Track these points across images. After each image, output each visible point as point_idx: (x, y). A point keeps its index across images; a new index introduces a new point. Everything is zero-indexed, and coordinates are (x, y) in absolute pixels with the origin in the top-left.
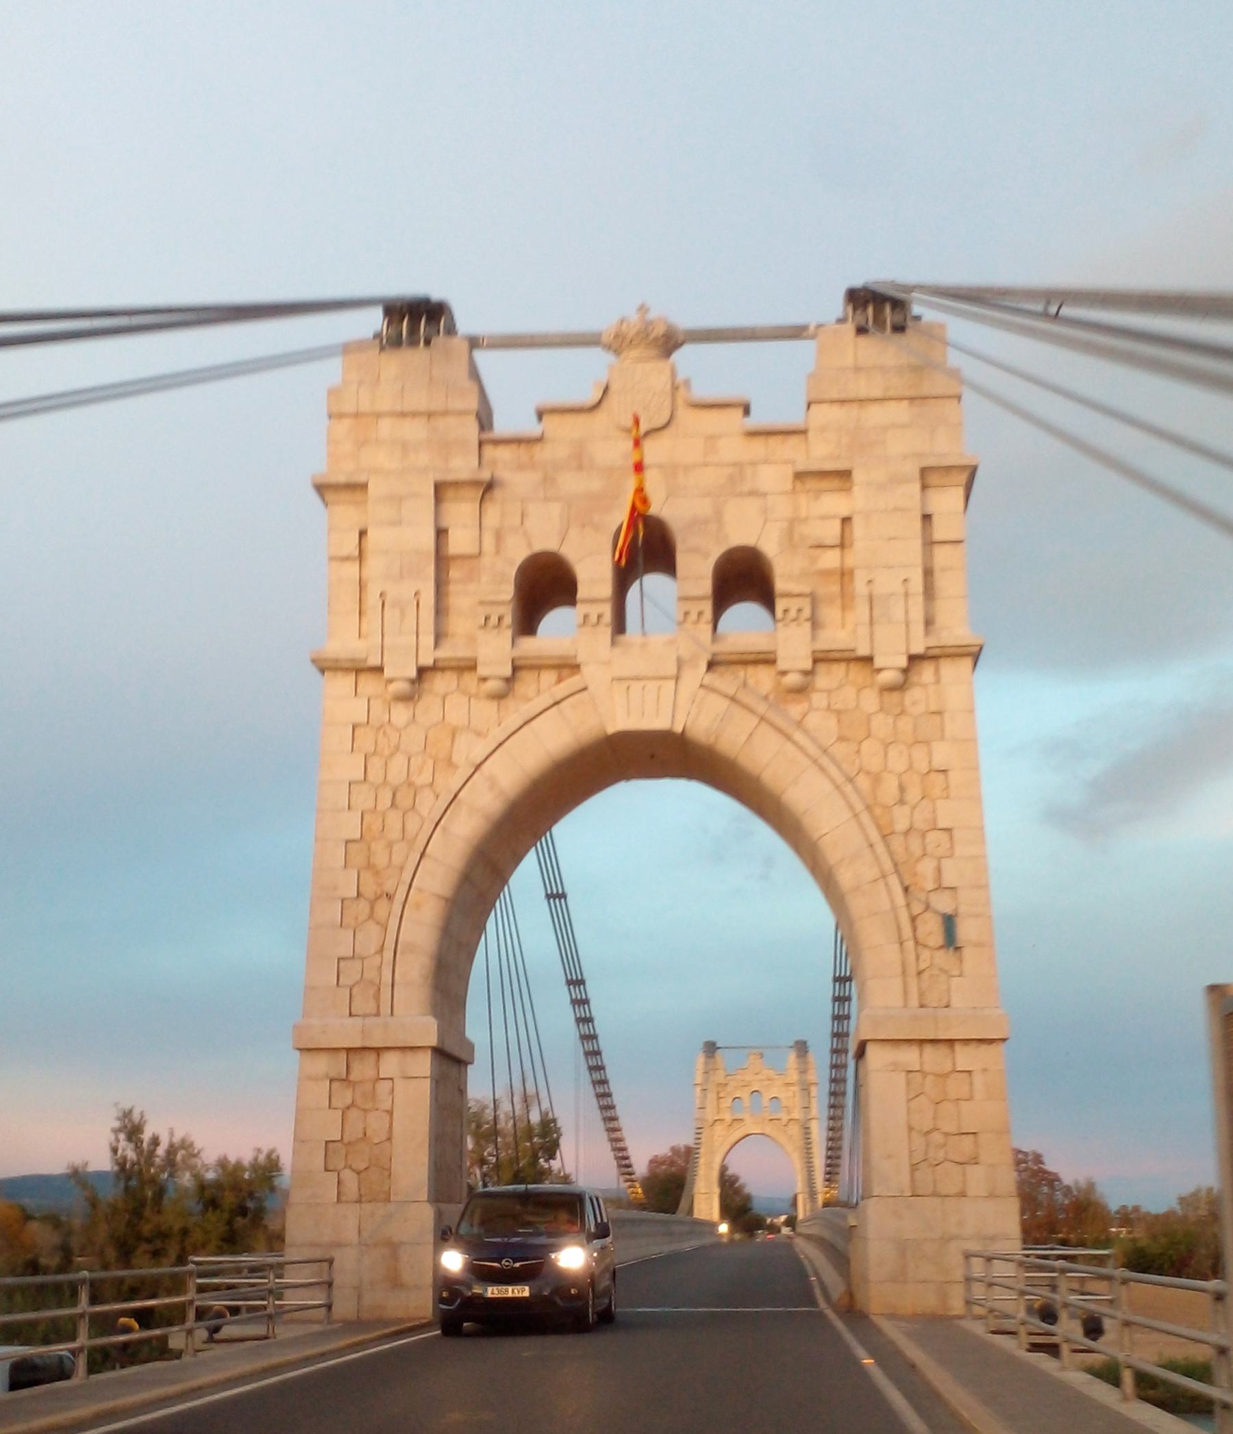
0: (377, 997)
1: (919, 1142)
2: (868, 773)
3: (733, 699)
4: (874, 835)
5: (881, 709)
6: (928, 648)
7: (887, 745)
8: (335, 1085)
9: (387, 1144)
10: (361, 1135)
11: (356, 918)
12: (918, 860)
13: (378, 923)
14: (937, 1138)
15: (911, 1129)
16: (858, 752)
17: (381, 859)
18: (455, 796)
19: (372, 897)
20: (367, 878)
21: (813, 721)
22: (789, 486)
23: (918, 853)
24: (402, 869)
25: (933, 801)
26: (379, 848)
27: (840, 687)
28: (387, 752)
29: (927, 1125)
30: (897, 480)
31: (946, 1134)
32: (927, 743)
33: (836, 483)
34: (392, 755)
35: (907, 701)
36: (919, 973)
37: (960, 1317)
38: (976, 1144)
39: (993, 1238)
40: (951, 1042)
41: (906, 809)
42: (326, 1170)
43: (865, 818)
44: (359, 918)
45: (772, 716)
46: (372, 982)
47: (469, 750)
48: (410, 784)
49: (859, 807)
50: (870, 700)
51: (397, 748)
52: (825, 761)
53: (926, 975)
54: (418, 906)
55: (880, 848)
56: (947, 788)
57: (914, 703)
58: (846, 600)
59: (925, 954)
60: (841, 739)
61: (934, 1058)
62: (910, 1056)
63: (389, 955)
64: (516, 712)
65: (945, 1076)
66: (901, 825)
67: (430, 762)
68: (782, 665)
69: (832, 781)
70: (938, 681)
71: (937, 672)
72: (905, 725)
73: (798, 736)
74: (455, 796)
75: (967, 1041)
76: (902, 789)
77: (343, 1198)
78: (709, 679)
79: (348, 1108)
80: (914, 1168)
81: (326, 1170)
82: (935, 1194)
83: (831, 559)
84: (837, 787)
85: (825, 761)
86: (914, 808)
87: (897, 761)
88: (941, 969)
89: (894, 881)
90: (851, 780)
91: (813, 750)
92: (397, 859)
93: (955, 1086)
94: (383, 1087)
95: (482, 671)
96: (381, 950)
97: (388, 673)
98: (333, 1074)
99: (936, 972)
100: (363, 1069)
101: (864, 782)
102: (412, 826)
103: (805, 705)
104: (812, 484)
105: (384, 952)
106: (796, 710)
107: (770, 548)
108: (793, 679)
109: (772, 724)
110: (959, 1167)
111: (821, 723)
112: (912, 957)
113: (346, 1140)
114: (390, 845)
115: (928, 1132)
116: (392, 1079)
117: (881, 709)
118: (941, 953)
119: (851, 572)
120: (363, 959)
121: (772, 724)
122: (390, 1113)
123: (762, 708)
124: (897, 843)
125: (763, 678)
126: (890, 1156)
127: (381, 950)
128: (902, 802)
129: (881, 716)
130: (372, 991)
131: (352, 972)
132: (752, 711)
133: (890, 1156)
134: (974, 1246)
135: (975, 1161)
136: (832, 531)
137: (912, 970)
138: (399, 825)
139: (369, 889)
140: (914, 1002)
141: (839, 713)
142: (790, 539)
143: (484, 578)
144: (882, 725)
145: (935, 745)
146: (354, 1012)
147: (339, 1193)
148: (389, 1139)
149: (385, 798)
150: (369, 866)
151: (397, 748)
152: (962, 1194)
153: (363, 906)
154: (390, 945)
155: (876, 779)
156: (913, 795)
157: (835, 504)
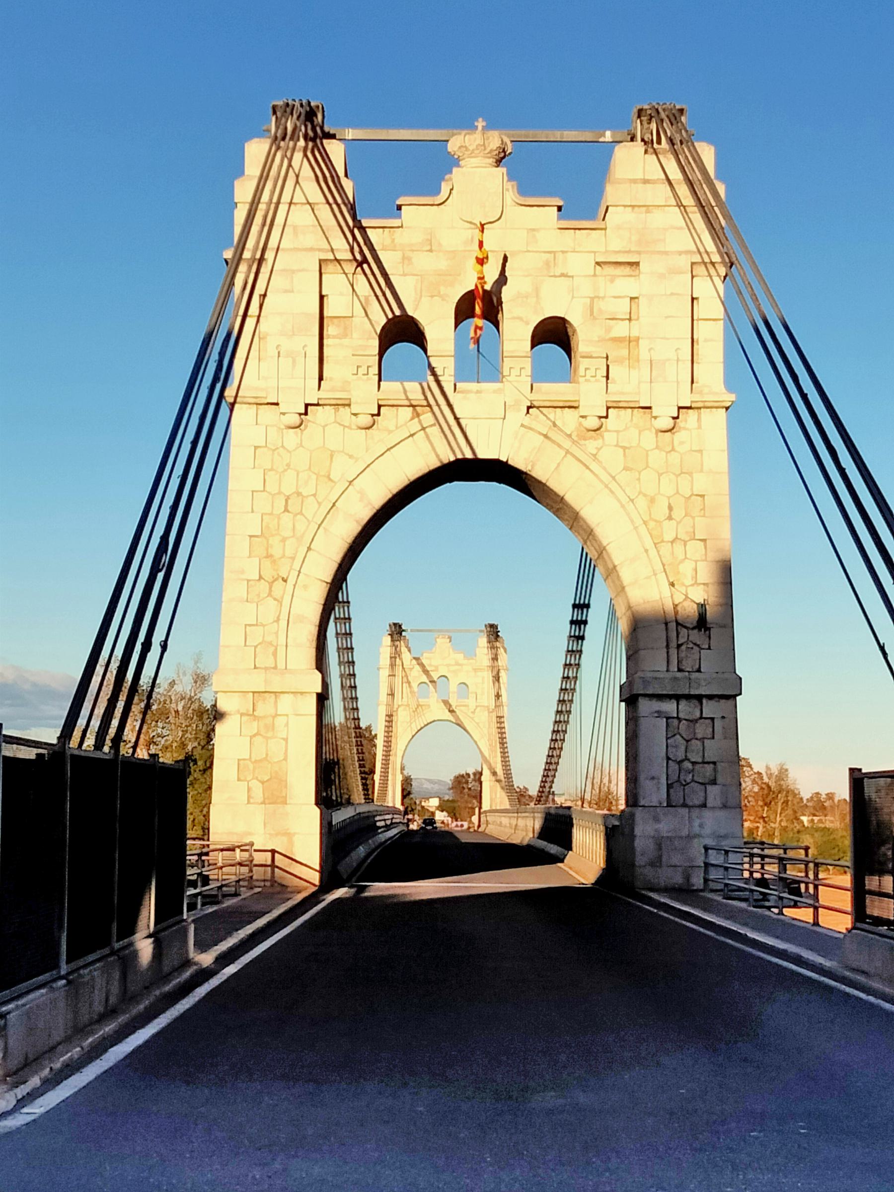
0: (275, 654)
1: (674, 766)
2: (645, 495)
3: (546, 436)
4: (649, 544)
5: (657, 447)
6: (692, 402)
7: (660, 475)
8: (245, 718)
9: (284, 762)
10: (264, 756)
11: (258, 595)
12: (682, 561)
13: (275, 599)
14: (687, 765)
15: (668, 759)
16: (639, 479)
17: (276, 551)
18: (334, 504)
19: (271, 580)
20: (267, 563)
21: (603, 455)
22: (592, 273)
23: (681, 557)
24: (293, 559)
25: (693, 518)
26: (275, 541)
27: (626, 429)
28: (280, 470)
29: (681, 755)
30: (675, 271)
31: (694, 763)
32: (690, 474)
33: (627, 270)
34: (285, 470)
35: (676, 443)
36: (679, 646)
37: (701, 891)
38: (715, 770)
39: (725, 837)
40: (699, 698)
41: (673, 523)
42: (239, 780)
43: (643, 530)
44: (261, 595)
45: (575, 450)
46: (270, 643)
47: (343, 468)
48: (299, 494)
49: (638, 522)
50: (649, 440)
51: (288, 465)
52: (613, 486)
53: (683, 647)
54: (305, 587)
55: (653, 552)
56: (704, 509)
57: (682, 443)
58: (632, 360)
59: (684, 632)
60: (626, 469)
61: (686, 709)
62: (670, 707)
63: (283, 623)
64: (380, 438)
65: (695, 721)
66: (669, 536)
67: (314, 477)
68: (582, 411)
69: (619, 501)
70: (699, 427)
71: (699, 419)
72: (674, 458)
73: (593, 466)
74: (334, 504)
75: (710, 697)
76: (670, 508)
77: (252, 801)
78: (527, 420)
79: (255, 735)
80: (669, 787)
81: (239, 780)
82: (685, 805)
83: (621, 329)
84: (623, 506)
85: (613, 486)
86: (678, 523)
87: (667, 488)
88: (695, 644)
89: (662, 577)
90: (632, 500)
91: (605, 478)
92: (289, 552)
93: (702, 729)
94: (280, 721)
95: (355, 409)
96: (278, 620)
97: (283, 407)
98: (243, 711)
99: (691, 645)
100: (265, 708)
101: (642, 503)
102: (301, 527)
103: (600, 441)
104: (610, 270)
105: (280, 622)
106: (591, 445)
107: (575, 318)
108: (593, 423)
109: (574, 456)
110: (703, 787)
111: (611, 457)
112: (673, 634)
113: (253, 760)
114: (284, 540)
115: (682, 761)
116: (287, 715)
117: (657, 447)
118: (696, 631)
119: (637, 339)
120: (264, 626)
121: (574, 456)
122: (286, 740)
123: (567, 444)
124: (665, 549)
125: (568, 419)
126: (653, 778)
127: (278, 620)
128: (670, 518)
129: (657, 451)
130: (273, 649)
131: (257, 634)
132: (559, 446)
133: (653, 778)
134: (710, 842)
135: (714, 782)
136: (623, 307)
137: (673, 644)
138: (290, 526)
139: (268, 574)
140: (674, 667)
141: (624, 448)
142: (591, 313)
143: (355, 335)
144: (657, 459)
145: (695, 475)
146: (257, 666)
147: (249, 797)
148: (285, 759)
149: (280, 504)
150: (269, 556)
151: (288, 465)
152: (704, 805)
153: (263, 586)
154: (284, 616)
155: (652, 500)
156: (678, 514)
157: (626, 285)
